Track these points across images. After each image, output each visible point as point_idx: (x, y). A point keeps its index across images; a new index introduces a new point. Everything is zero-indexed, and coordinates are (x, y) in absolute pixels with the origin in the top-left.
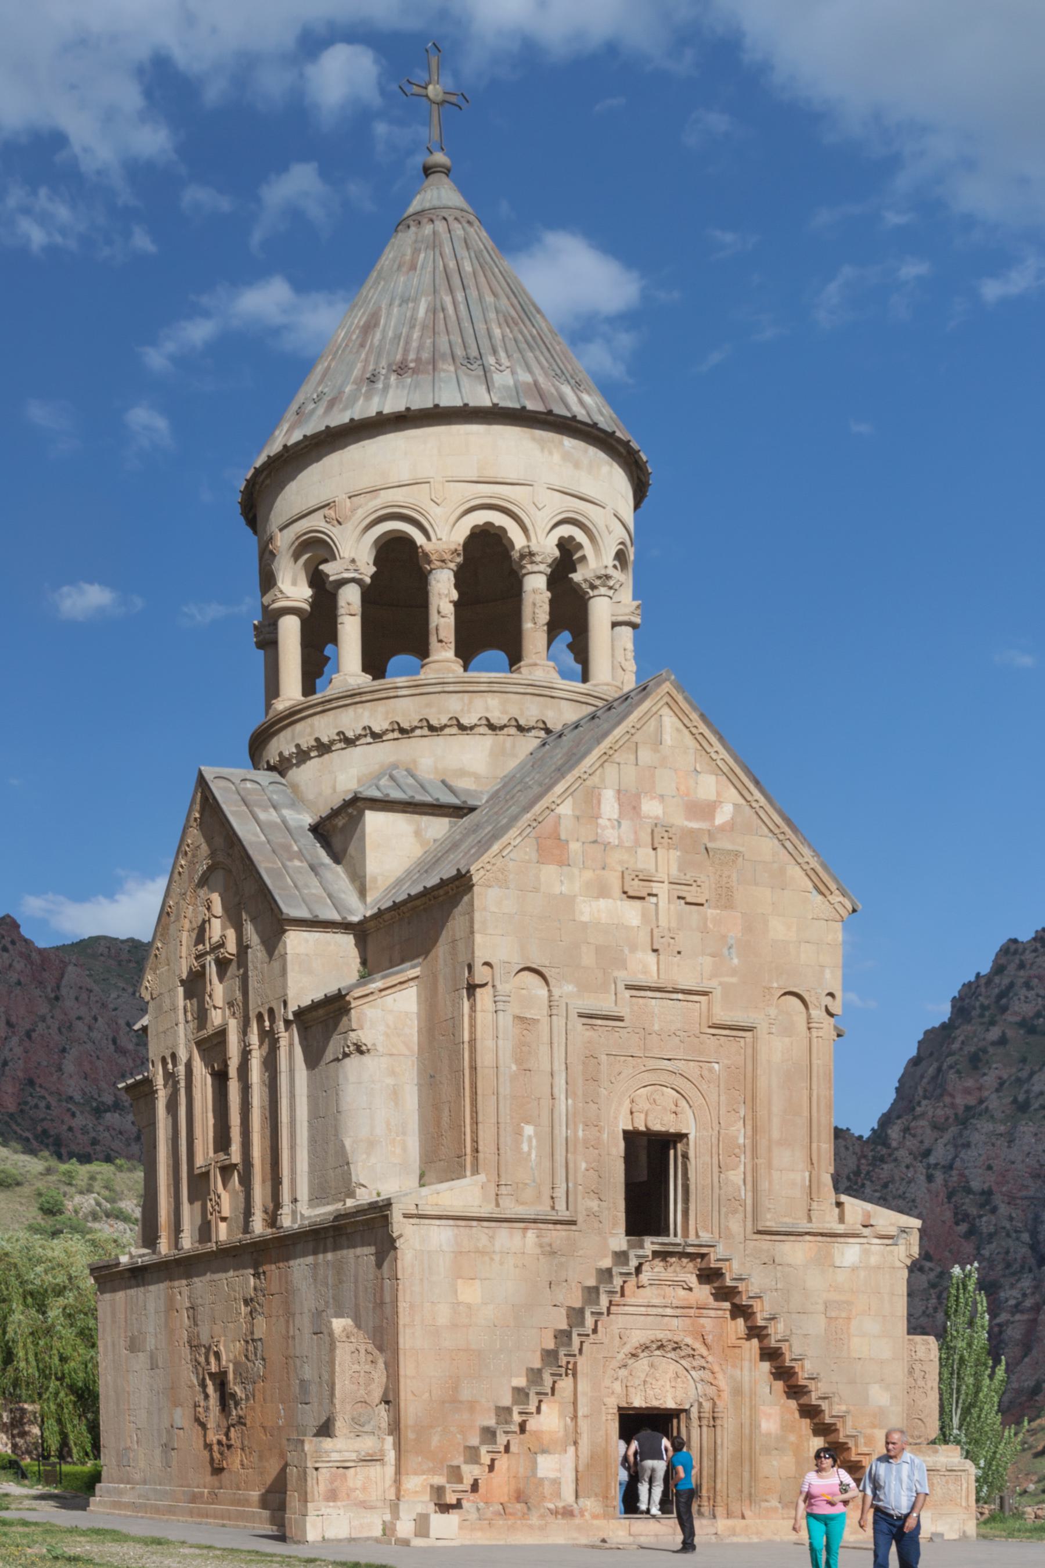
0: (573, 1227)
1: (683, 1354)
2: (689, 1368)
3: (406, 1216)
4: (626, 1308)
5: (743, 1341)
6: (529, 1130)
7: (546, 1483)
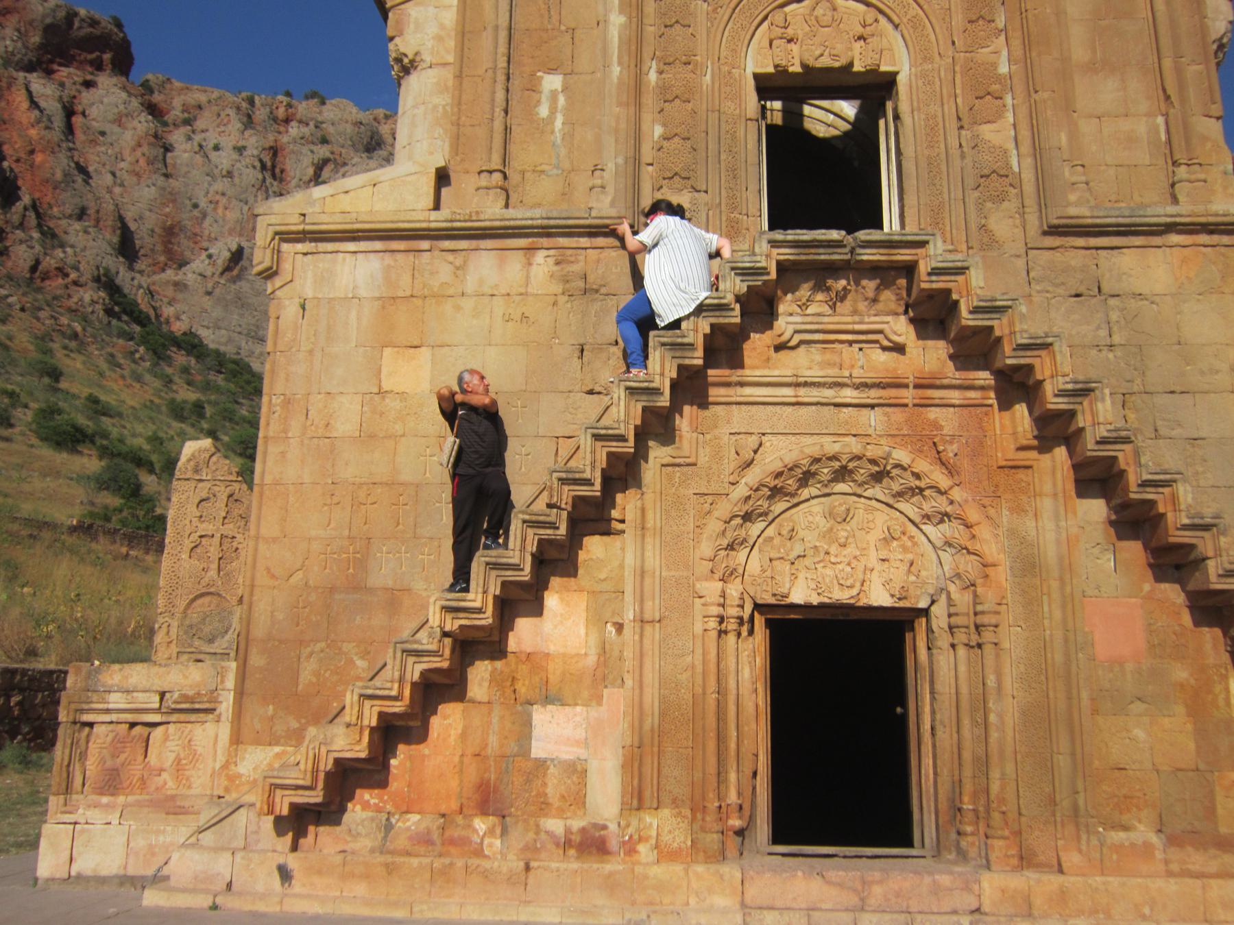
1: (896, 487)
2: (917, 520)
3: (287, 237)
4: (748, 391)
5: (1033, 454)
6: (552, 82)
7: (552, 770)
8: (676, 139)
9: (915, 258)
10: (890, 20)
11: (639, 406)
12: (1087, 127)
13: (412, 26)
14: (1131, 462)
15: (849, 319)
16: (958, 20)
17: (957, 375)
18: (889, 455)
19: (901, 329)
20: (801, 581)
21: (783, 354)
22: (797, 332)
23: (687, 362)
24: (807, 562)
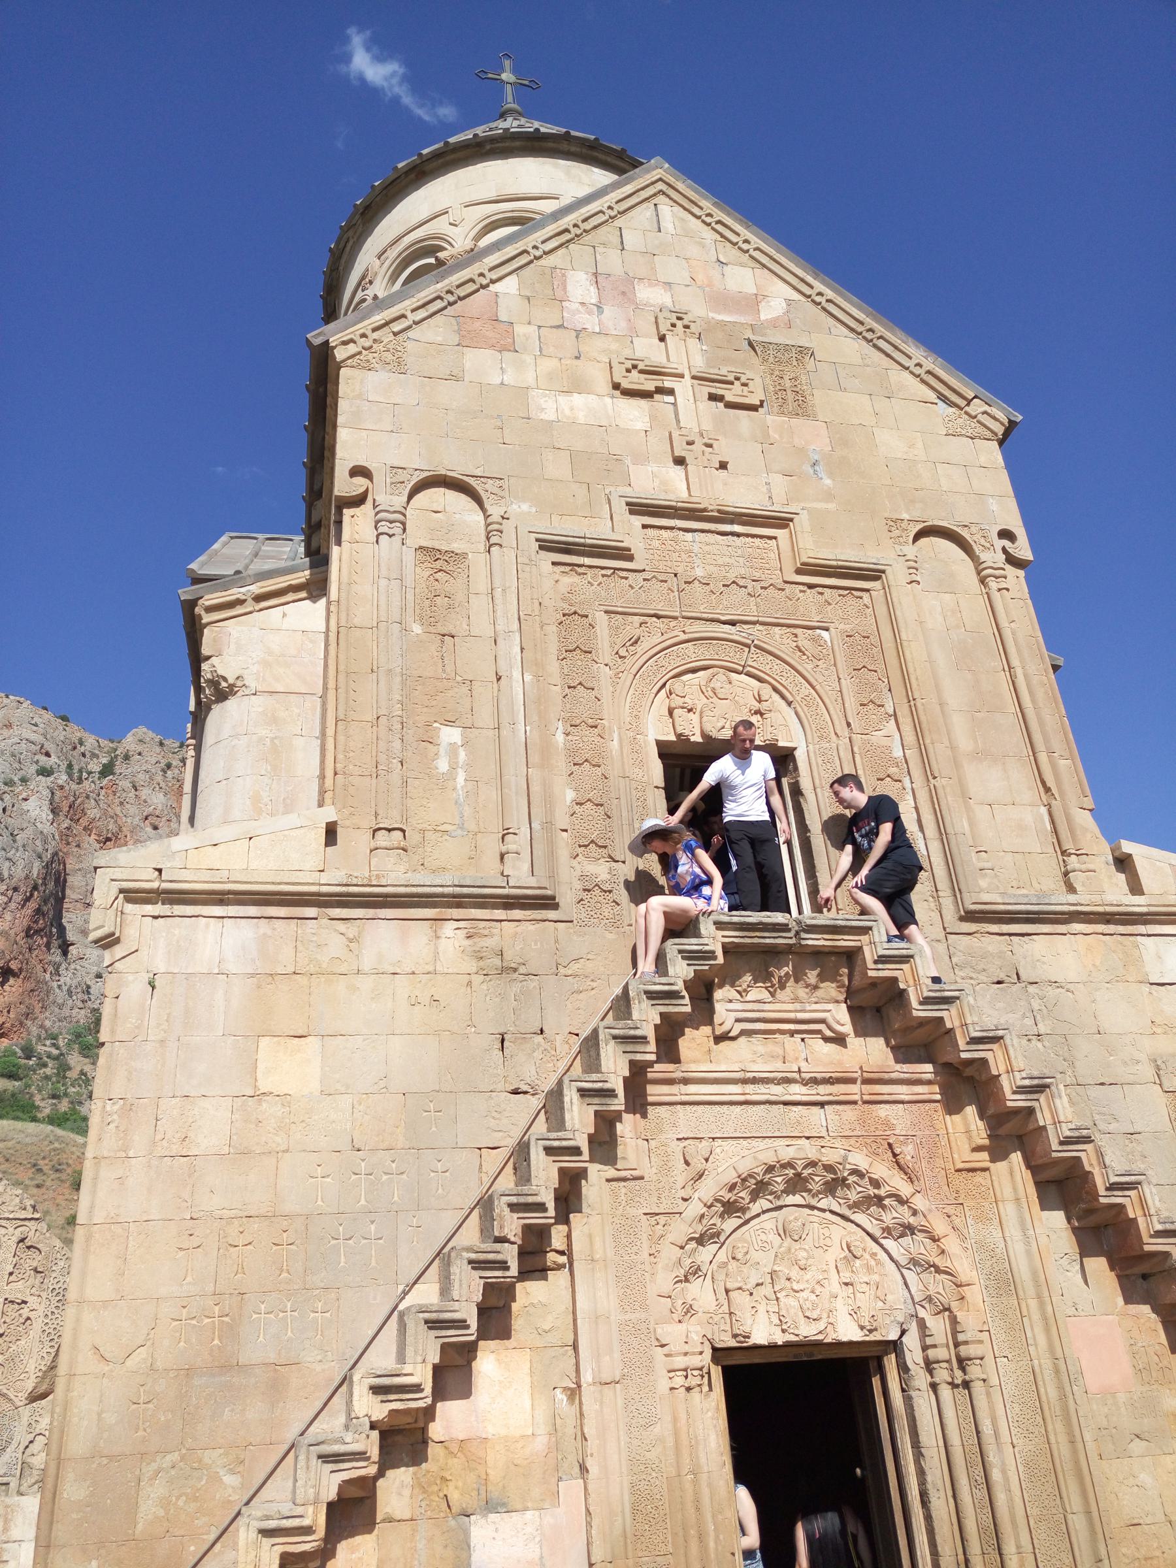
0: (551, 914)
1: (853, 1196)
2: (877, 1233)
3: (133, 896)
4: (692, 1088)
6: (450, 735)
8: (589, 805)
9: (858, 944)
10: (783, 697)
11: (591, 1110)
12: (982, 813)
13: (232, 646)
14: (1094, 1162)
15: (791, 1007)
16: (851, 704)
17: (898, 1067)
18: (845, 1158)
19: (841, 1017)
20: (762, 1315)
21: (724, 1045)
22: (738, 1020)
23: (639, 1057)
24: (767, 1290)
